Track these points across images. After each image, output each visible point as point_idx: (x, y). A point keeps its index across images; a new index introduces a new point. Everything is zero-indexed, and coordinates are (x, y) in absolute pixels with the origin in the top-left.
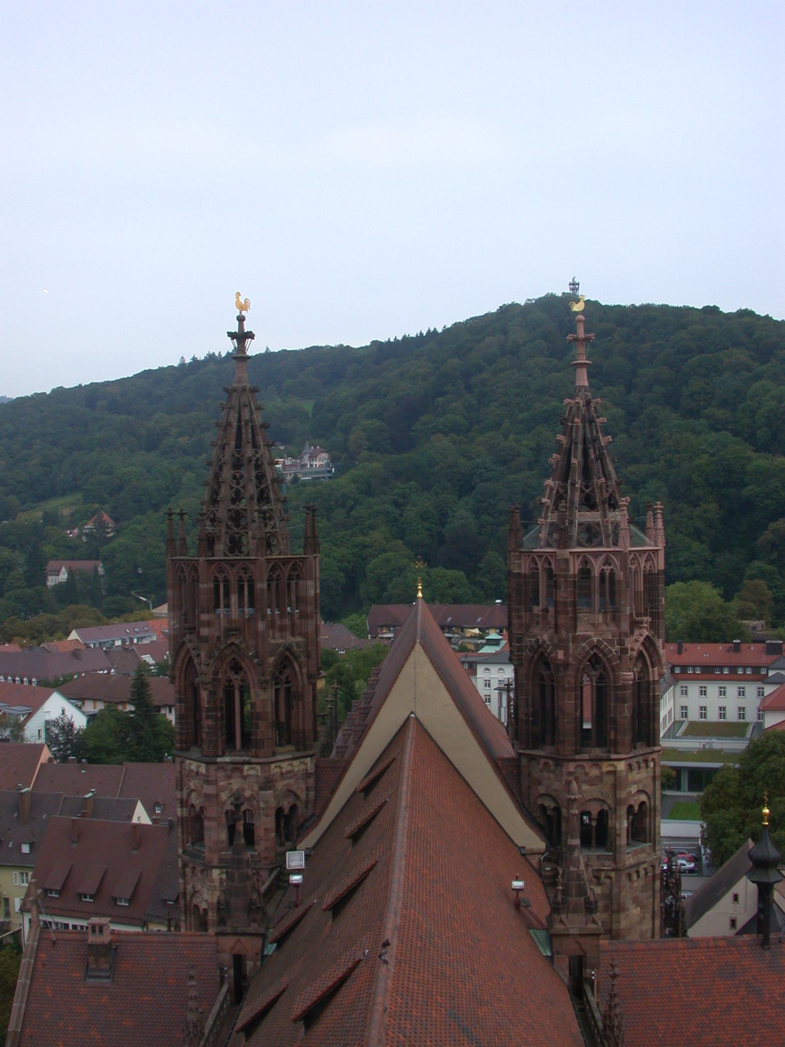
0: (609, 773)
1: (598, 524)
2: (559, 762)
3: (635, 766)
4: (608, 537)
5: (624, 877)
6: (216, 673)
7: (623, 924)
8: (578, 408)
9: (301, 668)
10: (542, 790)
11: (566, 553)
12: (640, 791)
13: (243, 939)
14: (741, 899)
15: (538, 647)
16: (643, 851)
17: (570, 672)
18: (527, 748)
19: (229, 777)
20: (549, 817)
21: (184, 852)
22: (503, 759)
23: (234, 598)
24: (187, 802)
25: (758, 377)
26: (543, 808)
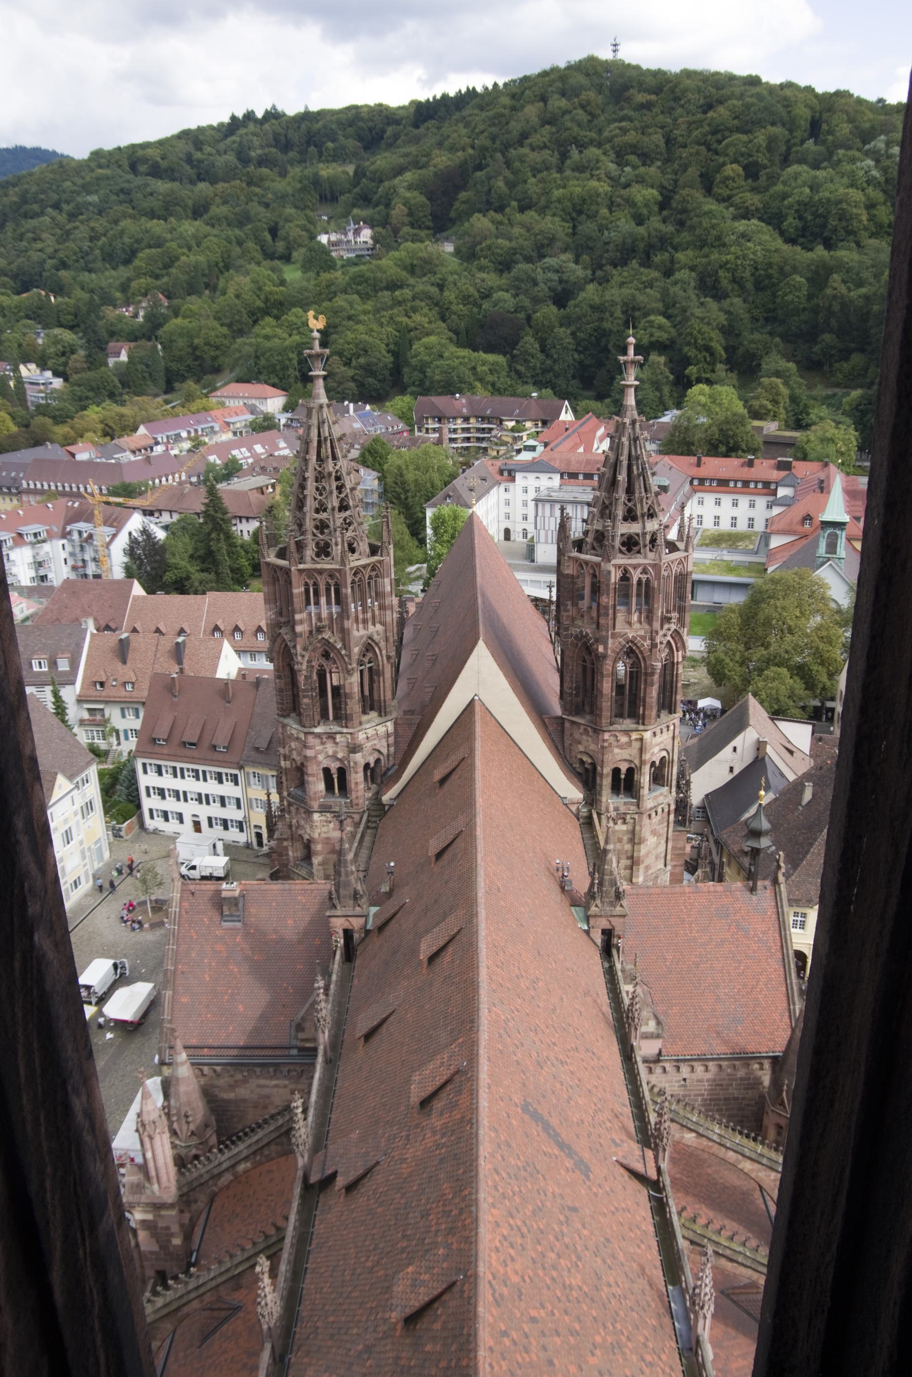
1: (638, 535)
3: (658, 732)
4: (645, 546)
5: (645, 817)
7: (643, 852)
10: (581, 748)
14: (738, 750)
15: (581, 637)
18: (570, 714)
20: (586, 769)
21: (289, 795)
23: (323, 600)
26: (582, 762)
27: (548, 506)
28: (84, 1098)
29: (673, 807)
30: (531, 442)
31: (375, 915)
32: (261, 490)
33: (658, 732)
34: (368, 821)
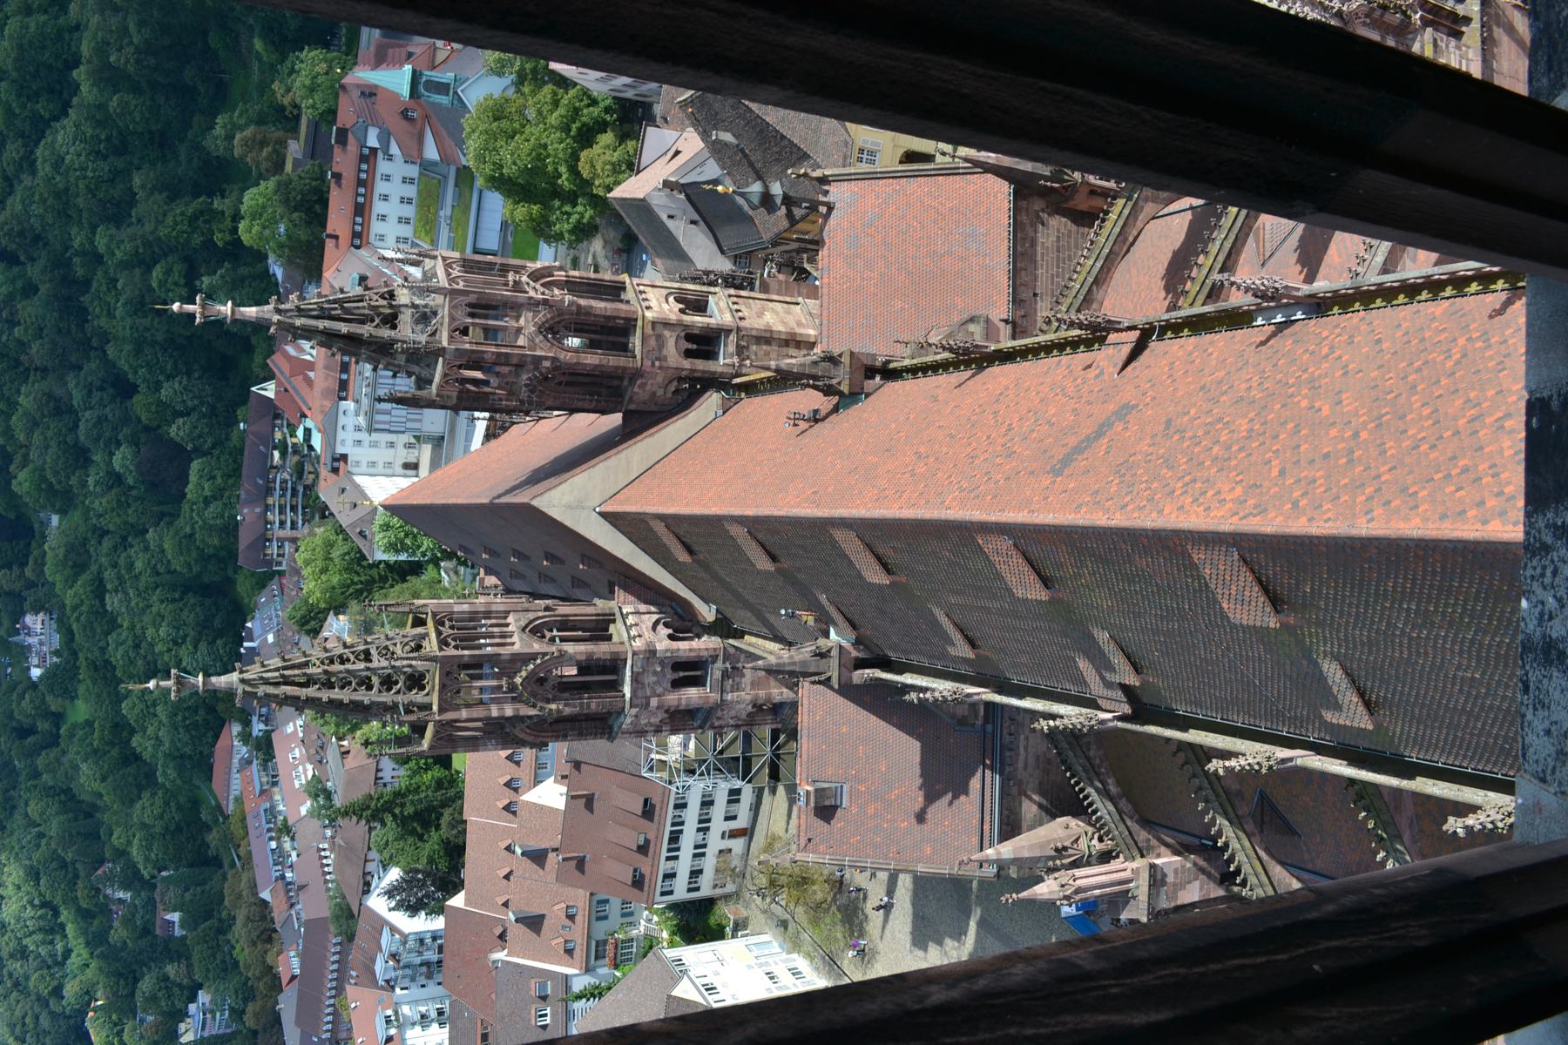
3: (644, 304)
7: (781, 328)
26: (677, 392)
28: (933, 988)
29: (732, 291)
30: (300, 433)
33: (644, 304)
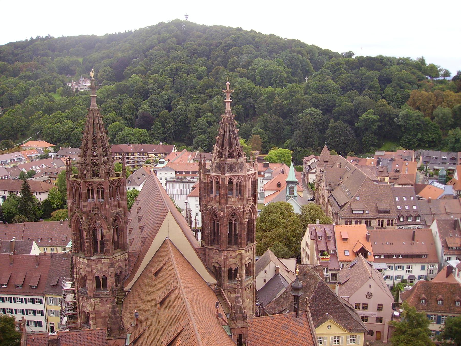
0: (238, 254)
1: (235, 163)
2: (220, 251)
6: (89, 225)
8: (227, 119)
9: (122, 220)
10: (214, 260)
11: (224, 176)
12: (249, 259)
13: (117, 340)
14: (267, 272)
16: (250, 279)
17: (225, 219)
19: (97, 264)
22: (198, 249)
23: (96, 196)
24: (78, 273)
25: (256, 57)
27: (171, 184)
30: (162, 160)
31: (130, 337)
32: (45, 181)
33: (247, 250)
34: (117, 301)
